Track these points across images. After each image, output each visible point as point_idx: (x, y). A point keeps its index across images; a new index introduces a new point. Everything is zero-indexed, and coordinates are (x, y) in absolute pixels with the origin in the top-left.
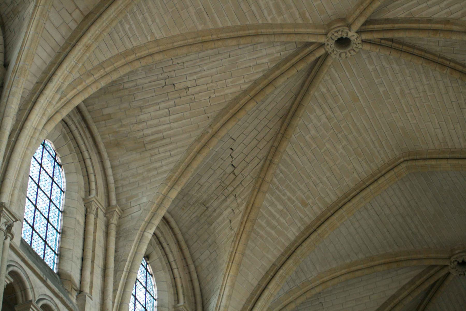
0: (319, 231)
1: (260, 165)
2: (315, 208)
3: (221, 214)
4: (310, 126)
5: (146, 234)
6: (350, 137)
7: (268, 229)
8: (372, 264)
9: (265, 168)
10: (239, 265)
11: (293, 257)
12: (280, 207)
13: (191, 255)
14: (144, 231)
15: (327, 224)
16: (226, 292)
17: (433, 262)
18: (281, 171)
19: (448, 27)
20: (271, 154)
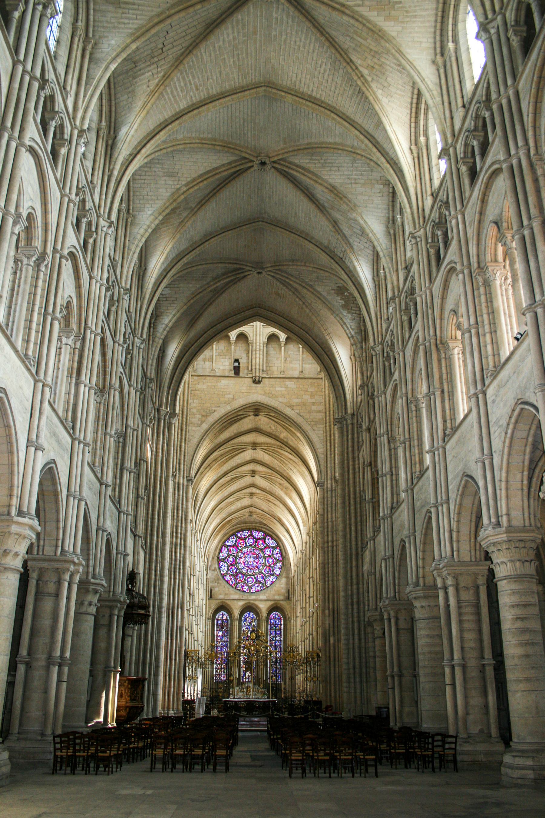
0: (200, 109)
1: (181, 51)
2: (202, 94)
3: (143, 74)
4: (221, 38)
5: (111, 66)
6: (240, 56)
7: (170, 95)
8: (214, 143)
9: (185, 55)
10: (148, 111)
11: (180, 120)
12: (182, 84)
13: (115, 94)
14: (110, 63)
15: (206, 107)
16: (135, 127)
17: (247, 156)
18: (192, 61)
19: (343, 9)
20: (192, 47)
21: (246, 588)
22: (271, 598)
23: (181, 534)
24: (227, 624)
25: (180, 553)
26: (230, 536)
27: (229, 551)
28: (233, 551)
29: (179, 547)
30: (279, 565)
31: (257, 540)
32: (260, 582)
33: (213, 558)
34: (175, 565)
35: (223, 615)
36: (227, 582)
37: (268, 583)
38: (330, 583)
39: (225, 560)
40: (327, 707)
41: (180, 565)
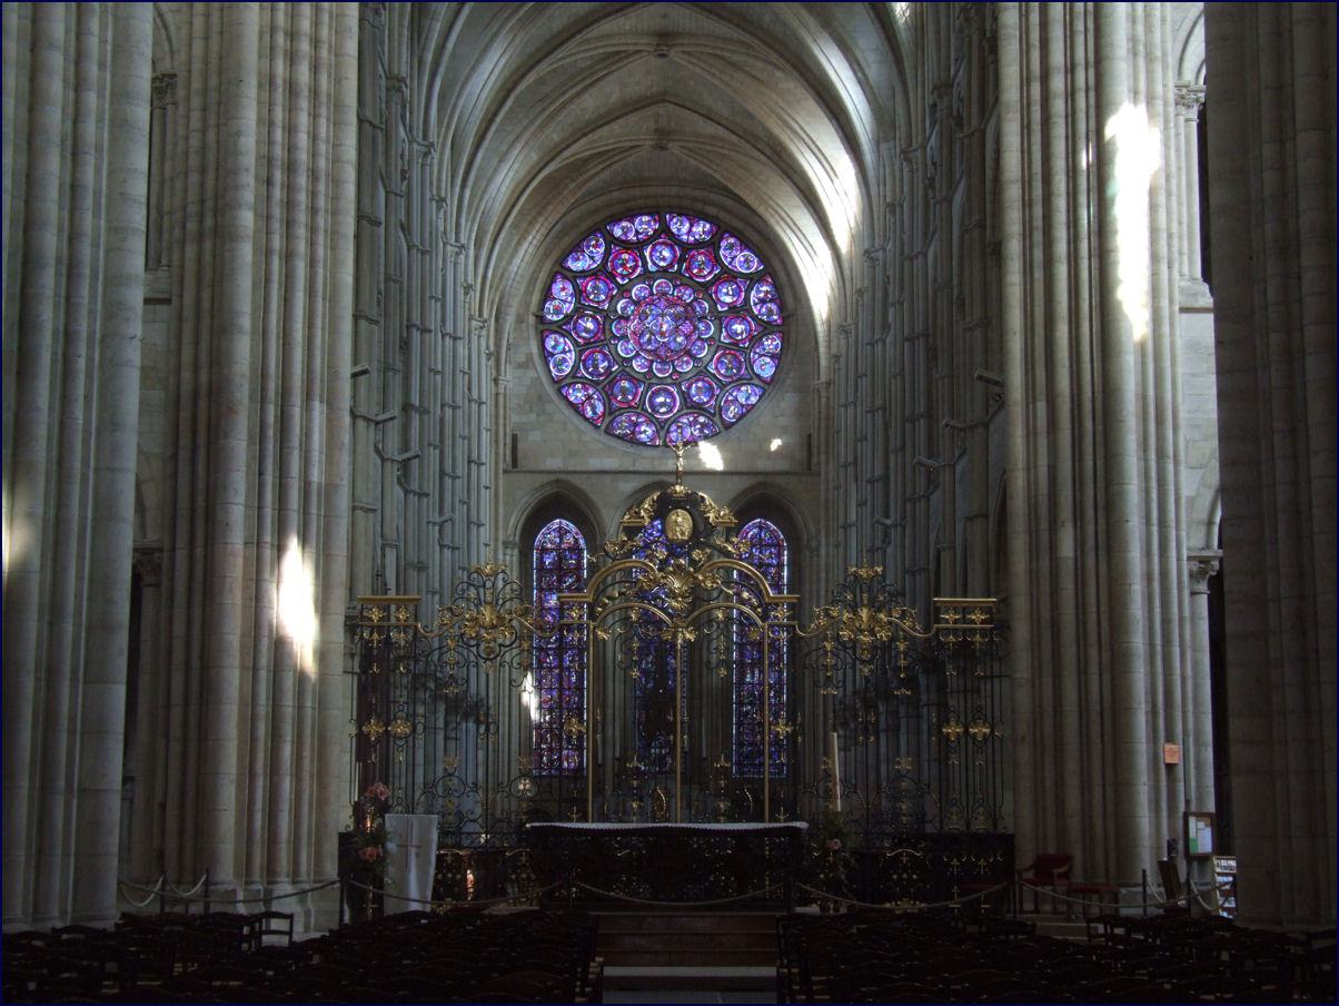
21: (647, 431)
22: (742, 467)
23: (316, 43)
24: (579, 566)
25: (314, 137)
26: (585, 237)
27: (579, 293)
28: (597, 292)
29: (304, 104)
30: (771, 344)
31: (687, 248)
32: (699, 408)
33: (520, 320)
34: (290, 188)
35: (562, 532)
36: (577, 409)
37: (732, 411)
38: (1062, 271)
39: (565, 327)
40: (1047, 867)
41: (313, 194)
